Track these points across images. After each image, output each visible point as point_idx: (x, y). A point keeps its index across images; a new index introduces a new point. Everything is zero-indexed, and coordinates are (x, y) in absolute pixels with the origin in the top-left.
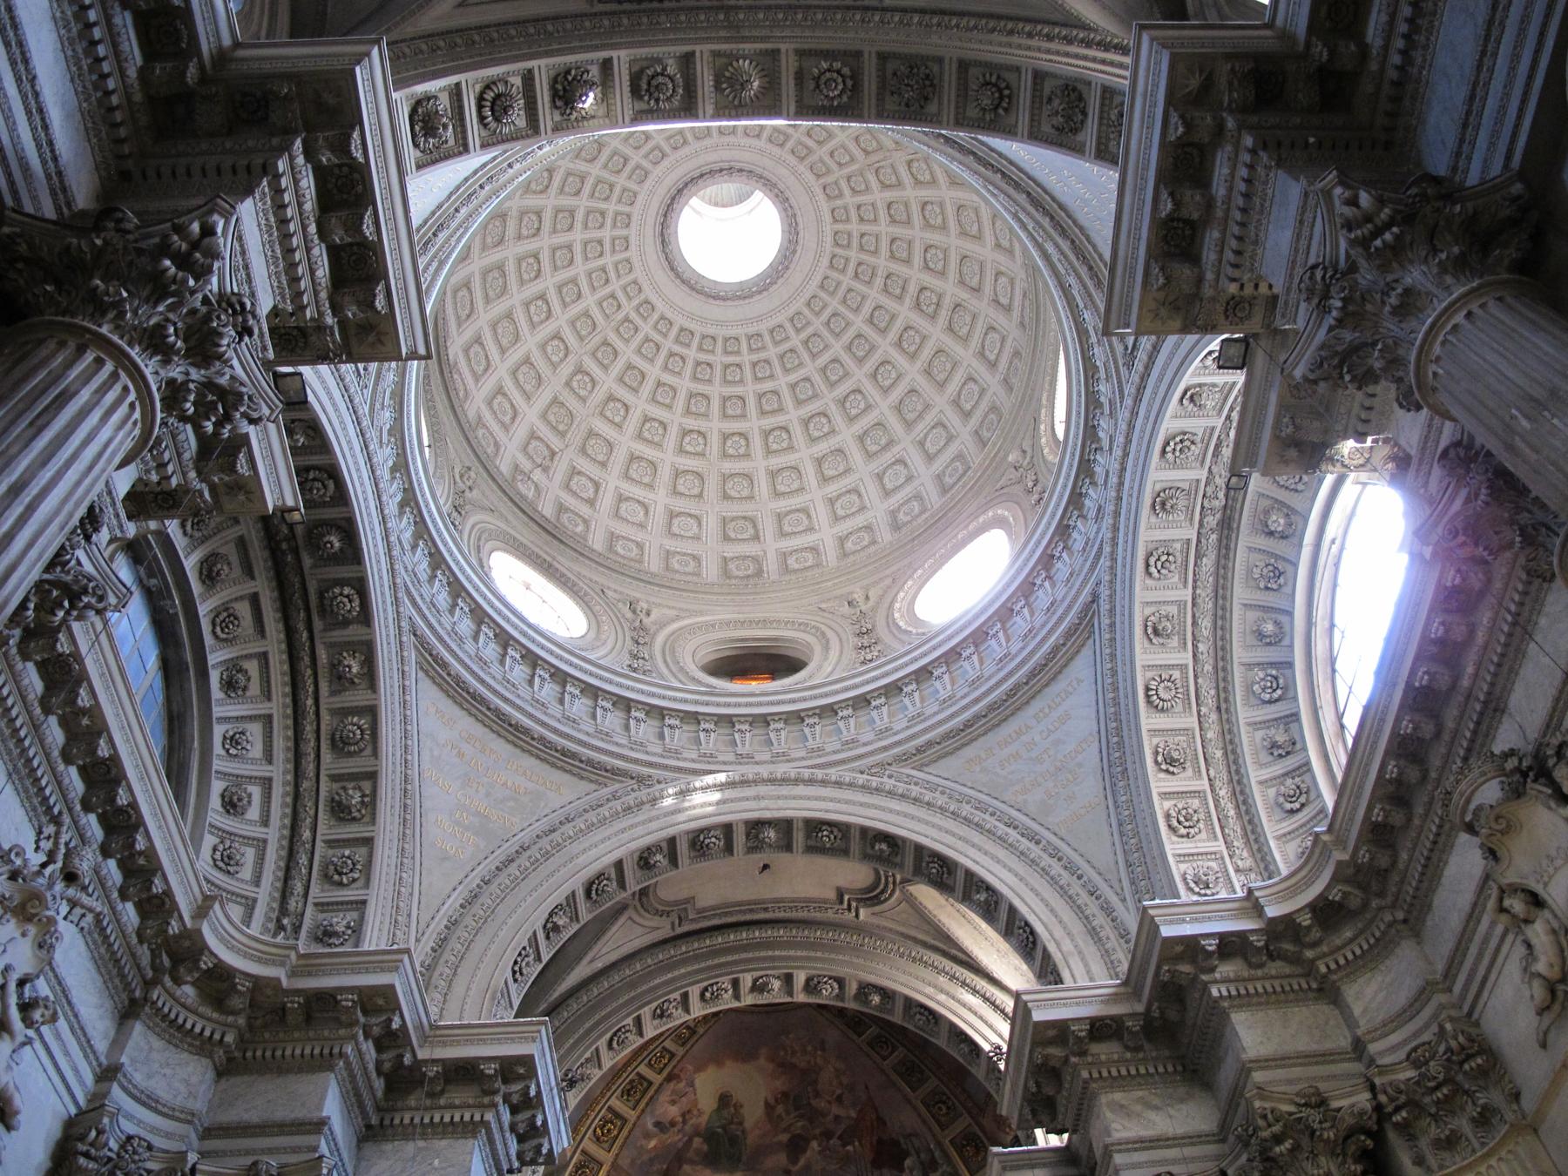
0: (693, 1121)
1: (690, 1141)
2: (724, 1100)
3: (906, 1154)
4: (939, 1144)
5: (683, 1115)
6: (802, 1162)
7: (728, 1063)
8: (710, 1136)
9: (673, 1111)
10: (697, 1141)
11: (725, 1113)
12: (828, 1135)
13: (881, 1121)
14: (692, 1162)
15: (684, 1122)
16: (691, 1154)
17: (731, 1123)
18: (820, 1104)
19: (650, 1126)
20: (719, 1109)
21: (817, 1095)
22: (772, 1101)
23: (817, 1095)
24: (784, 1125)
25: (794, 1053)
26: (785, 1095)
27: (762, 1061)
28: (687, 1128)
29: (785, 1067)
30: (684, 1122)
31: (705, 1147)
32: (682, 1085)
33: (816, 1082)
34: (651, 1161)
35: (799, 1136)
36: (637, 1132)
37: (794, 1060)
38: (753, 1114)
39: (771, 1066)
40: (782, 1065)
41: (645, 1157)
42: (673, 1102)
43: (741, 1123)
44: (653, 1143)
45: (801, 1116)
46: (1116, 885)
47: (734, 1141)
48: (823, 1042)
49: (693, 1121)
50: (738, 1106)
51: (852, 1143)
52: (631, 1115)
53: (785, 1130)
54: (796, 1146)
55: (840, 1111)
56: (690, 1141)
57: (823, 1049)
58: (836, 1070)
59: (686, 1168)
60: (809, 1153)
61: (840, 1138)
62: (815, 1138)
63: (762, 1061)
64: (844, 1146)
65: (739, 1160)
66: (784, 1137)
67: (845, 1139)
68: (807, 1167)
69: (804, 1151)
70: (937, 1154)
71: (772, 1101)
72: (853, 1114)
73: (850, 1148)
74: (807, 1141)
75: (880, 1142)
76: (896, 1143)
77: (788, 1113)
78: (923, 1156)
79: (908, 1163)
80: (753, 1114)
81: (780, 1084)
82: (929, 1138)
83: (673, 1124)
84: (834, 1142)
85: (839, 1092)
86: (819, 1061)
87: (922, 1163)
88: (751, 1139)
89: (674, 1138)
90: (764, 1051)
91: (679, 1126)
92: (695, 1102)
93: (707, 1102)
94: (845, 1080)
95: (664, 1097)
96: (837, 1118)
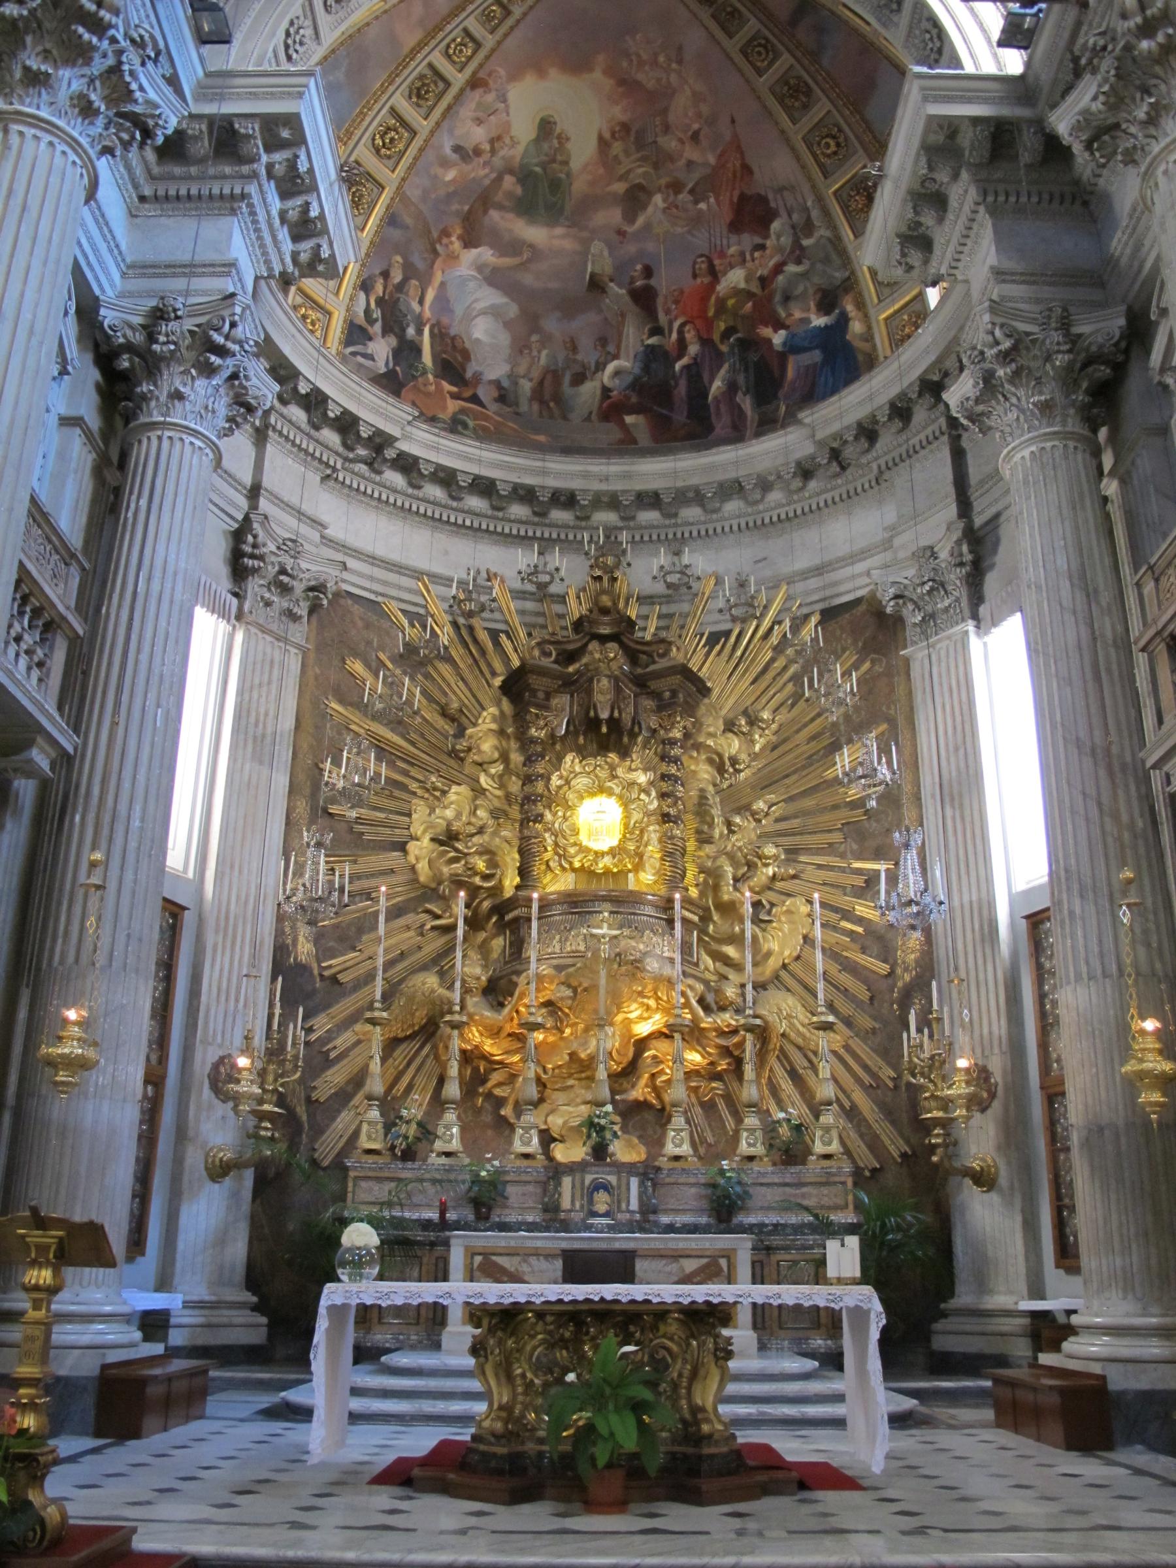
1: (499, 179)
2: (546, 127)
3: (771, 215)
4: (820, 200)
5: (492, 141)
6: (641, 221)
7: (553, 72)
8: (525, 176)
9: (478, 135)
10: (509, 182)
11: (546, 146)
12: (676, 187)
13: (747, 170)
14: (500, 207)
15: (493, 151)
16: (499, 197)
17: (554, 161)
18: (670, 143)
19: (448, 150)
20: (538, 140)
21: (667, 129)
22: (607, 135)
23: (667, 129)
24: (622, 170)
25: (641, 64)
26: (625, 127)
27: (597, 75)
29: (627, 85)
30: (493, 151)
31: (519, 190)
32: (490, 97)
33: (665, 111)
34: (450, 197)
35: (640, 187)
36: (430, 155)
37: (640, 77)
39: (612, 82)
40: (622, 82)
41: (442, 192)
42: (479, 121)
43: (566, 163)
44: (450, 175)
45: (644, 159)
47: (555, 185)
48: (680, 49)
50: (563, 139)
51: (705, 199)
52: (423, 126)
53: (621, 178)
54: (635, 199)
56: (499, 179)
57: (680, 62)
58: (694, 93)
59: (494, 214)
60: (650, 209)
61: (691, 192)
62: (659, 190)
63: (597, 75)
64: (696, 202)
65: (561, 211)
66: (620, 187)
67: (697, 194)
68: (648, 227)
69: (644, 207)
70: (815, 214)
71: (607, 135)
72: (712, 160)
73: (702, 206)
74: (650, 194)
75: (743, 197)
76: (763, 200)
77: (627, 153)
78: (795, 216)
79: (775, 226)
81: (618, 112)
83: (477, 152)
84: (684, 197)
85: (696, 126)
86: (673, 78)
87: (793, 227)
88: (579, 186)
89: (479, 171)
90: (601, 58)
91: (486, 157)
92: (507, 126)
93: (523, 130)
94: (705, 109)
95: (467, 111)
96: (690, 164)
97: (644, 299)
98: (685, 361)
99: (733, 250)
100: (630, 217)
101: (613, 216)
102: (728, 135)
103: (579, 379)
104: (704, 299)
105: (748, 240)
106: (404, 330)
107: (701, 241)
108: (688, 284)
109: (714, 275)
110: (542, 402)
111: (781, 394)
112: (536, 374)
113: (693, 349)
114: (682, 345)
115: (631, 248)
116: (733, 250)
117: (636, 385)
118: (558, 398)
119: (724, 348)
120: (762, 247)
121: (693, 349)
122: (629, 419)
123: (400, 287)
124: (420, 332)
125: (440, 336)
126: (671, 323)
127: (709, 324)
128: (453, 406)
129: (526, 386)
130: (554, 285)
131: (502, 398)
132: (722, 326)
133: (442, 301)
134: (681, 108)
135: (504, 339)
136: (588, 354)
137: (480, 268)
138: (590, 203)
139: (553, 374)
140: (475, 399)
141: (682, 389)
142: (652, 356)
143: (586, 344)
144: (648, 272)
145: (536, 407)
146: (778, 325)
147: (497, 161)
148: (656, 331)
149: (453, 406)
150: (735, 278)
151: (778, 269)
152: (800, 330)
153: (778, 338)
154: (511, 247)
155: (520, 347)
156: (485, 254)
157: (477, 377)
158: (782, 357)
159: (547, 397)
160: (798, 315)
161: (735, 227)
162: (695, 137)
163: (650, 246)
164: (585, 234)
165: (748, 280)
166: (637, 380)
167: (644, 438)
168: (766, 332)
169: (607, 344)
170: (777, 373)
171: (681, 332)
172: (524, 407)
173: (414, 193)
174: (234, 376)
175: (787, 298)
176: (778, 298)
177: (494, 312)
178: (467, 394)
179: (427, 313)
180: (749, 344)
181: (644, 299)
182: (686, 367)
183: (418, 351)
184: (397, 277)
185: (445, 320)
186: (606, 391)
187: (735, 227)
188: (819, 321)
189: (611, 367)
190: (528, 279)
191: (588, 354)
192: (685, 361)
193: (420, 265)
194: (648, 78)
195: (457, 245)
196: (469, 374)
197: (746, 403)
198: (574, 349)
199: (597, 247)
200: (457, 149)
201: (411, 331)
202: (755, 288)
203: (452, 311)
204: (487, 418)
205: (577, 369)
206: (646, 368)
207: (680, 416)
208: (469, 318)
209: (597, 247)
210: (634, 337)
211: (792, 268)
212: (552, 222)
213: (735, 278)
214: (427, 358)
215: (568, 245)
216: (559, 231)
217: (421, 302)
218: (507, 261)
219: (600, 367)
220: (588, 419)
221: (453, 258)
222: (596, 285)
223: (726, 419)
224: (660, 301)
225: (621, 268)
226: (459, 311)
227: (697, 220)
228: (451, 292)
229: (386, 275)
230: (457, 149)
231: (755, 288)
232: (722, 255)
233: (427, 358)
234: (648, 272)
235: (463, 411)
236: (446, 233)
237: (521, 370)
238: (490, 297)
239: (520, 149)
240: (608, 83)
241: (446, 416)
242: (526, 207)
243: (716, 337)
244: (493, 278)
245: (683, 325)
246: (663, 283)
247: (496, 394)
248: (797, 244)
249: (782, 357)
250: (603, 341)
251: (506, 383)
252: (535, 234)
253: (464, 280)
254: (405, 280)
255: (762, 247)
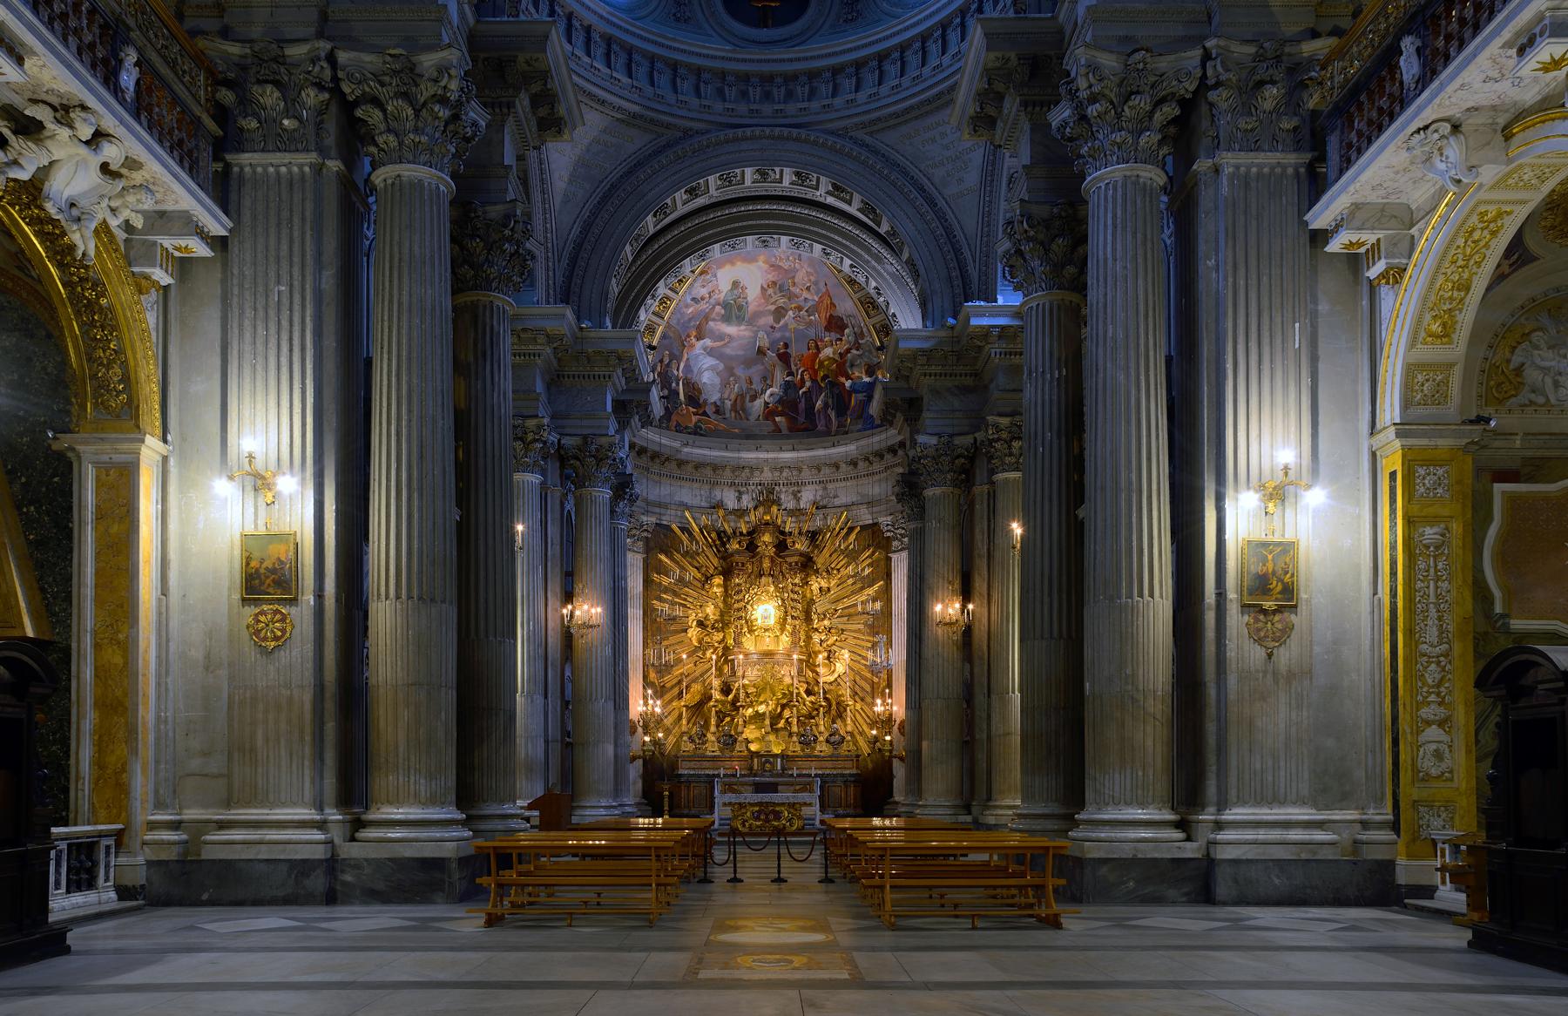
0: (716, 296)
1: (714, 307)
2: (736, 284)
3: (846, 326)
5: (710, 293)
7: (739, 263)
8: (726, 305)
9: (704, 292)
10: (718, 308)
11: (735, 292)
12: (800, 308)
13: (833, 305)
14: (714, 320)
15: (710, 297)
16: (714, 315)
18: (796, 290)
19: (689, 301)
22: (765, 286)
26: (774, 283)
27: (760, 263)
28: (712, 301)
31: (723, 311)
33: (794, 277)
34: (690, 320)
38: (753, 293)
40: (772, 266)
42: (704, 286)
43: (746, 298)
44: (690, 310)
46: (973, 250)
47: (740, 308)
49: (716, 296)
55: (808, 296)
59: (711, 324)
63: (760, 263)
66: (773, 308)
68: (786, 325)
70: (865, 330)
71: (765, 286)
73: (812, 317)
74: (787, 311)
77: (775, 294)
79: (847, 331)
80: (753, 293)
81: (771, 277)
82: (861, 319)
83: (703, 299)
88: (752, 308)
89: (703, 306)
94: (813, 279)
95: (697, 284)
97: (784, 358)
98: (804, 389)
99: (826, 339)
100: (777, 320)
101: (770, 320)
102: (824, 290)
103: (754, 398)
104: (813, 361)
105: (834, 336)
106: (670, 385)
107: (812, 333)
108: (805, 352)
109: (819, 350)
110: (736, 411)
111: (848, 413)
112: (733, 397)
113: (808, 384)
114: (803, 381)
115: (778, 335)
116: (826, 339)
117: (780, 401)
118: (744, 410)
119: (823, 385)
120: (841, 340)
121: (808, 384)
122: (777, 419)
123: (668, 365)
124: (678, 384)
125: (687, 383)
126: (797, 371)
127: (816, 372)
128: (694, 419)
129: (728, 404)
130: (741, 353)
131: (717, 412)
132: (822, 374)
133: (688, 368)
134: (801, 277)
135: (717, 380)
136: (757, 386)
137: (705, 349)
138: (757, 315)
139: (741, 396)
140: (705, 414)
141: (802, 405)
142: (787, 386)
143: (756, 379)
144: (786, 346)
145: (733, 414)
146: (848, 378)
147: (712, 301)
148: (790, 374)
149: (694, 419)
150: (828, 352)
151: (848, 351)
152: (858, 381)
153: (848, 384)
154: (720, 337)
155: (725, 384)
156: (708, 342)
157: (705, 401)
158: (850, 393)
159: (738, 408)
160: (857, 374)
161: (828, 328)
162: (808, 288)
163: (787, 334)
164: (755, 328)
165: (834, 353)
166: (781, 398)
167: (784, 431)
168: (843, 380)
169: (767, 380)
170: (847, 400)
171: (802, 375)
172: (728, 415)
173: (673, 322)
174: (631, 495)
175: (852, 366)
176: (848, 364)
177: (712, 368)
178: (701, 412)
179: (681, 374)
180: (835, 385)
181: (784, 358)
182: (804, 393)
183: (678, 394)
184: (666, 361)
185: (689, 376)
186: (766, 404)
187: (828, 328)
188: (867, 379)
189: (768, 392)
190: (728, 351)
191: (757, 386)
192: (804, 389)
193: (677, 353)
194: (786, 265)
195: (694, 340)
196: (701, 401)
197: (833, 415)
198: (751, 383)
199: (761, 334)
200: (693, 299)
201: (674, 385)
202: (837, 357)
203: (692, 371)
204: (710, 423)
205: (752, 393)
206: (786, 392)
207: (802, 419)
208: (700, 373)
209: (761, 334)
210: (780, 376)
211: (854, 351)
212: (739, 324)
213: (828, 352)
214: (682, 397)
215: (747, 333)
216: (743, 327)
217: (678, 370)
218: (718, 344)
219: (763, 392)
220: (758, 419)
221: (692, 346)
222: (761, 352)
223: (823, 422)
224: (792, 359)
225: (773, 343)
226: (695, 370)
227: (810, 323)
228: (692, 363)
229: (661, 361)
230: (693, 299)
231: (837, 357)
232: (822, 340)
233: (682, 397)
234: (786, 346)
235: (699, 421)
236: (689, 336)
237: (726, 396)
238: (709, 362)
239: (723, 294)
240: (766, 267)
241: (691, 425)
242: (727, 319)
243: (819, 380)
244: (710, 352)
245: (803, 372)
246: (793, 351)
247: (714, 410)
248: (856, 341)
249: (850, 393)
250: (765, 378)
251: (718, 403)
252: (731, 330)
253: (697, 356)
254: (670, 361)
255: (841, 340)
